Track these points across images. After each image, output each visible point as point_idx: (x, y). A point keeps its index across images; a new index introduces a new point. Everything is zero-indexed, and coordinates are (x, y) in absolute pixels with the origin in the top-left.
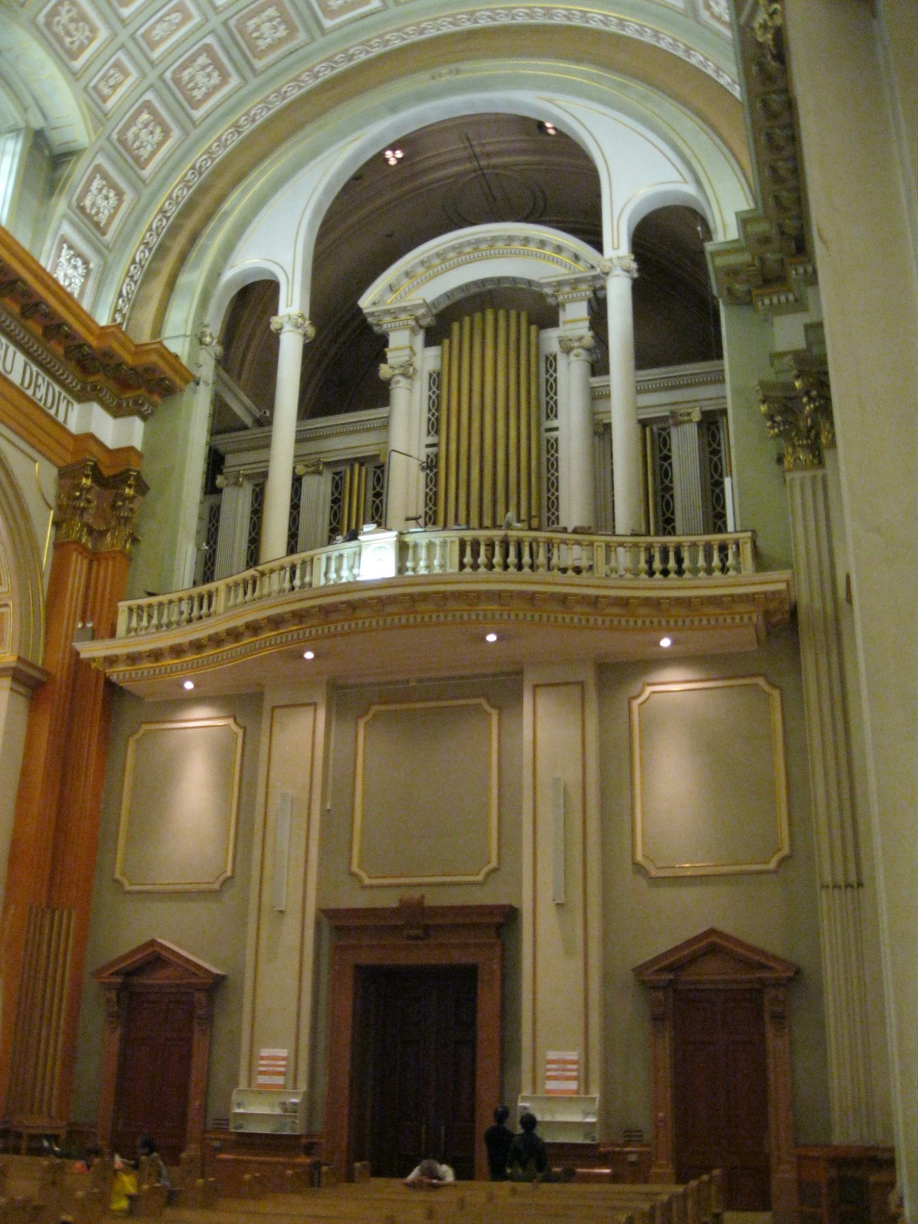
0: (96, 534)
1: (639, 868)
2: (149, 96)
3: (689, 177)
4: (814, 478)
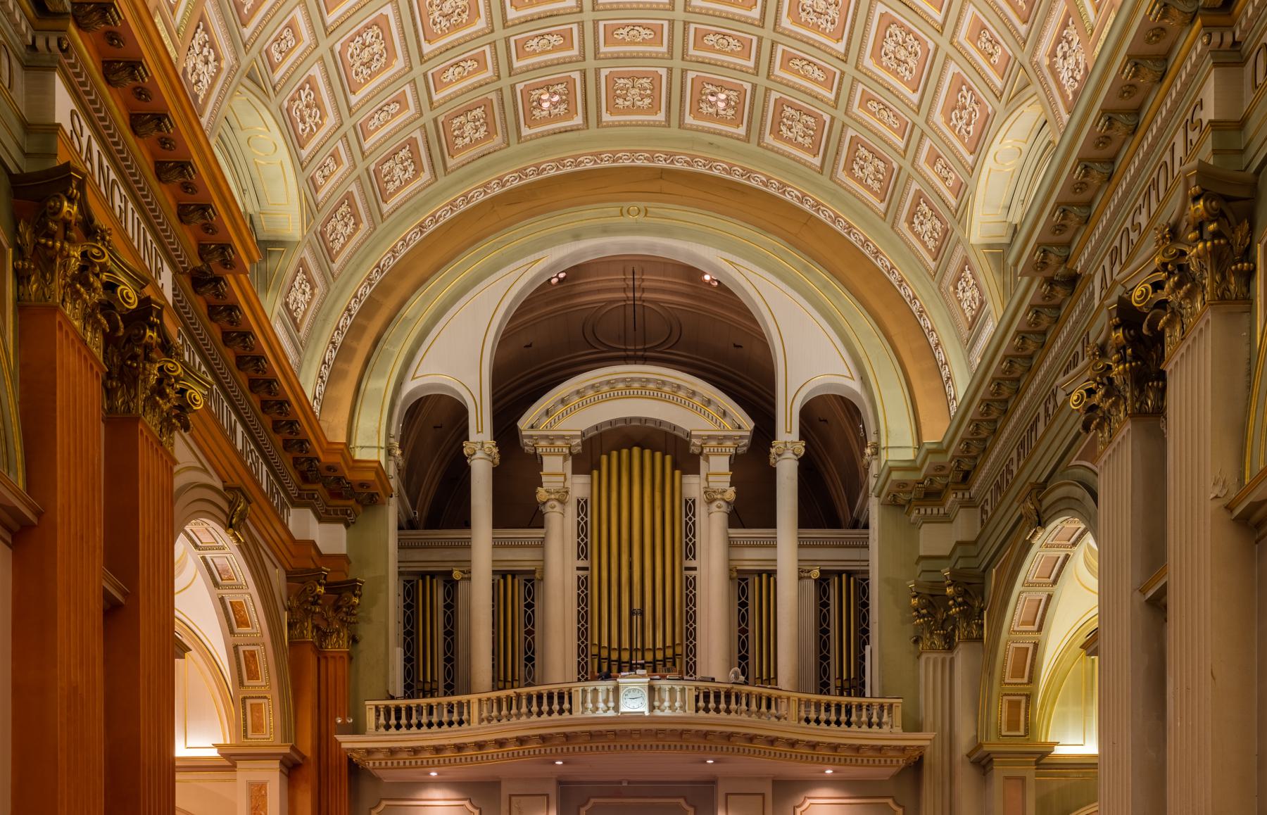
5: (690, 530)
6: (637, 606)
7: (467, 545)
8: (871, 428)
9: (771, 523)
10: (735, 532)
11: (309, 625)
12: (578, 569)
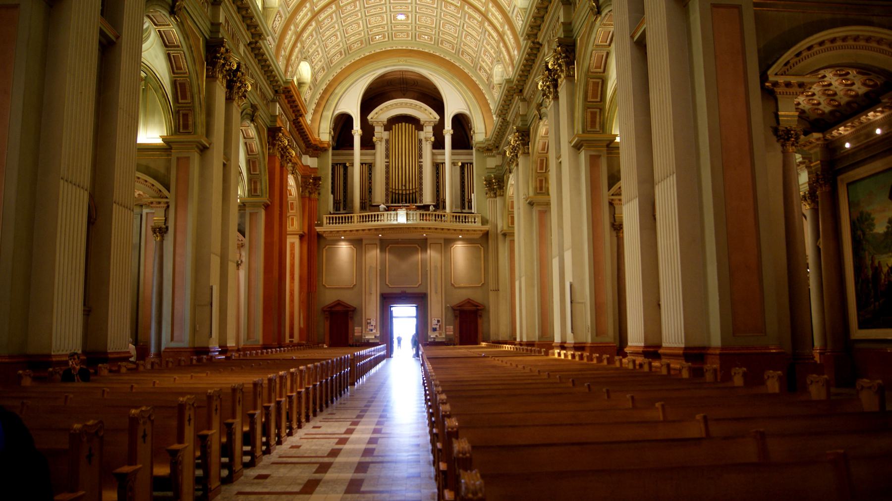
0: (310, 193)
1: (452, 285)
2: (324, 66)
4: (494, 201)
5: (420, 149)
7: (352, 155)
8: (473, 126)
9: (444, 148)
10: (435, 151)
11: (307, 191)
12: (386, 162)
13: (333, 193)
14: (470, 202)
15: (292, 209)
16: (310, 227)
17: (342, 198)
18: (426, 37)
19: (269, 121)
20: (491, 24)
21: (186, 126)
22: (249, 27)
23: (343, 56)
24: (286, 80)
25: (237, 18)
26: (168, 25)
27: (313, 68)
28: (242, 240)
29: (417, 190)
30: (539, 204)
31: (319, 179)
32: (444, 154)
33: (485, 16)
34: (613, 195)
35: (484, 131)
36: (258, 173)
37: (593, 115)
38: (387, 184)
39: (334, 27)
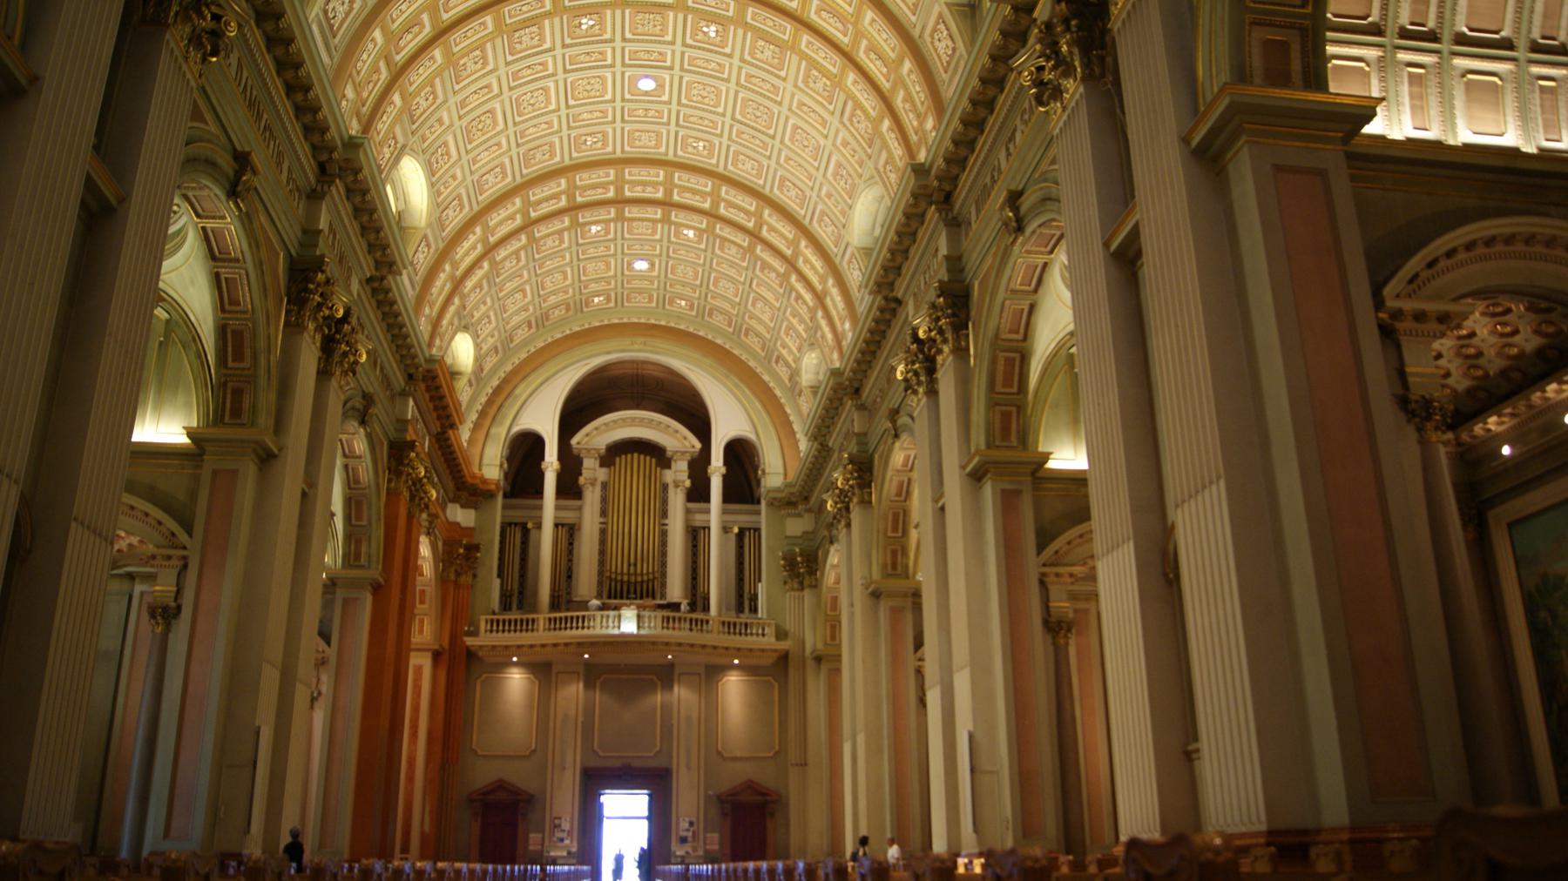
0: (458, 574)
1: (719, 753)
3: (753, 430)
5: (665, 501)
6: (632, 561)
7: (540, 508)
9: (707, 500)
10: (691, 505)
11: (453, 570)
13: (499, 576)
14: (754, 598)
15: (422, 602)
16: (455, 637)
17: (516, 586)
18: (683, 303)
19: (392, 428)
20: (802, 277)
21: (237, 412)
22: (371, 248)
23: (533, 330)
24: (431, 356)
25: (352, 227)
26: (223, 218)
27: (477, 346)
28: (323, 652)
29: (656, 575)
30: (891, 595)
31: (477, 548)
32: (708, 511)
33: (791, 263)
34: (1044, 565)
35: (781, 470)
36: (365, 523)
37: (1006, 417)
38: (602, 563)
39: (521, 276)
